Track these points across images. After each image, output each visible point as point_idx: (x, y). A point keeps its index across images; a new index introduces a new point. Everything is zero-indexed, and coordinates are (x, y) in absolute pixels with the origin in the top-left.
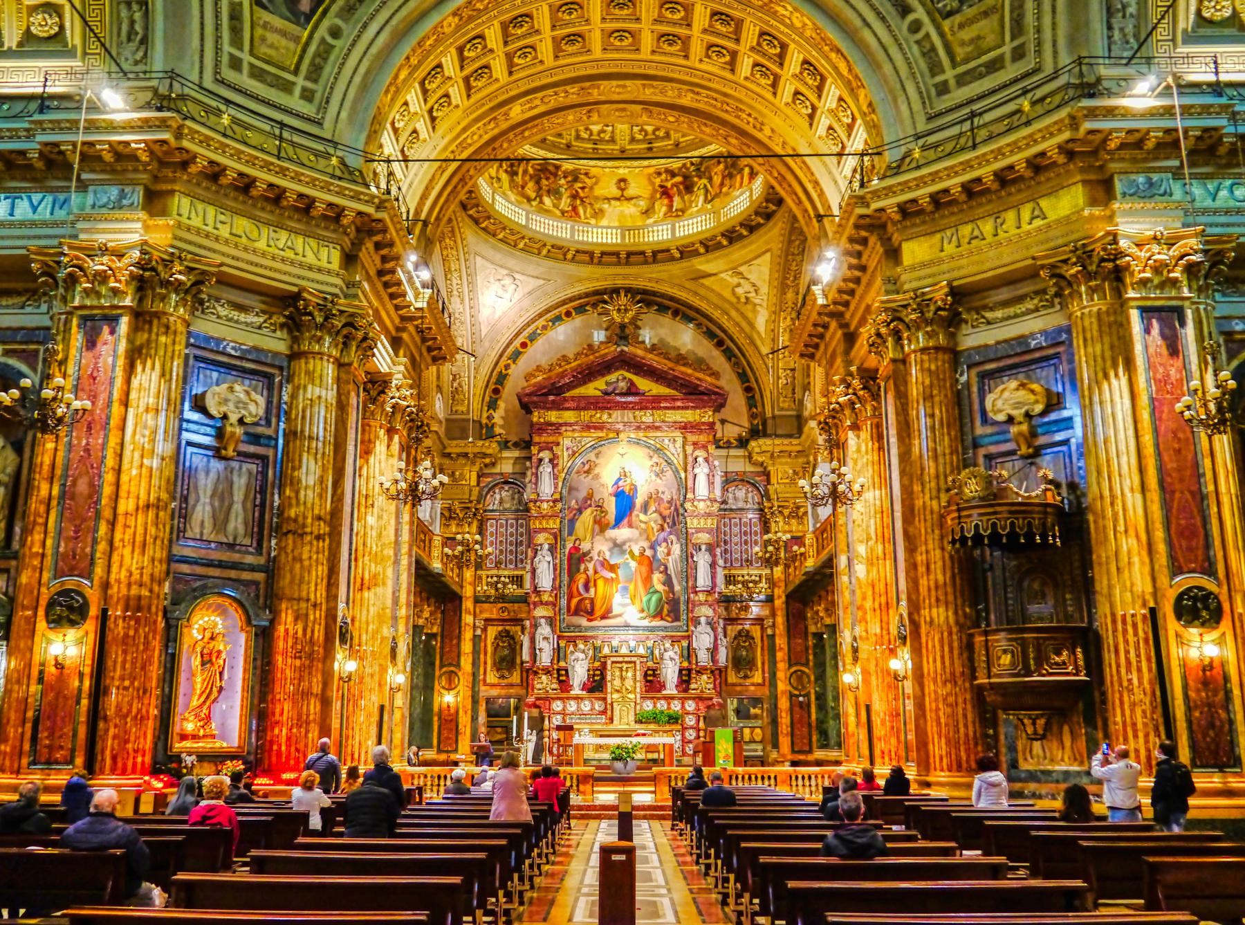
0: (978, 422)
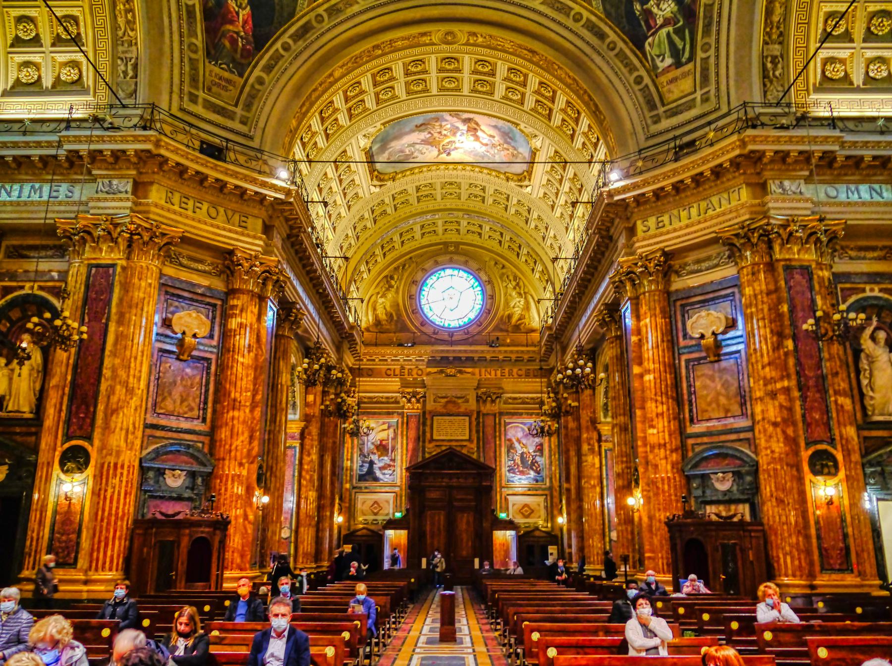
0: (681, 339)
